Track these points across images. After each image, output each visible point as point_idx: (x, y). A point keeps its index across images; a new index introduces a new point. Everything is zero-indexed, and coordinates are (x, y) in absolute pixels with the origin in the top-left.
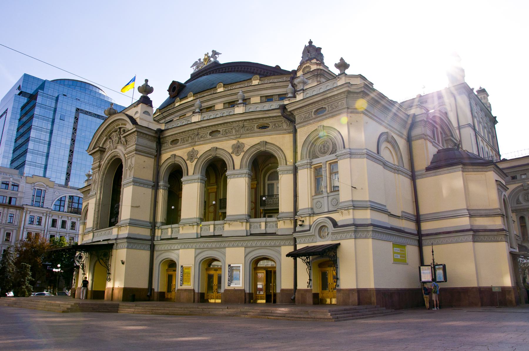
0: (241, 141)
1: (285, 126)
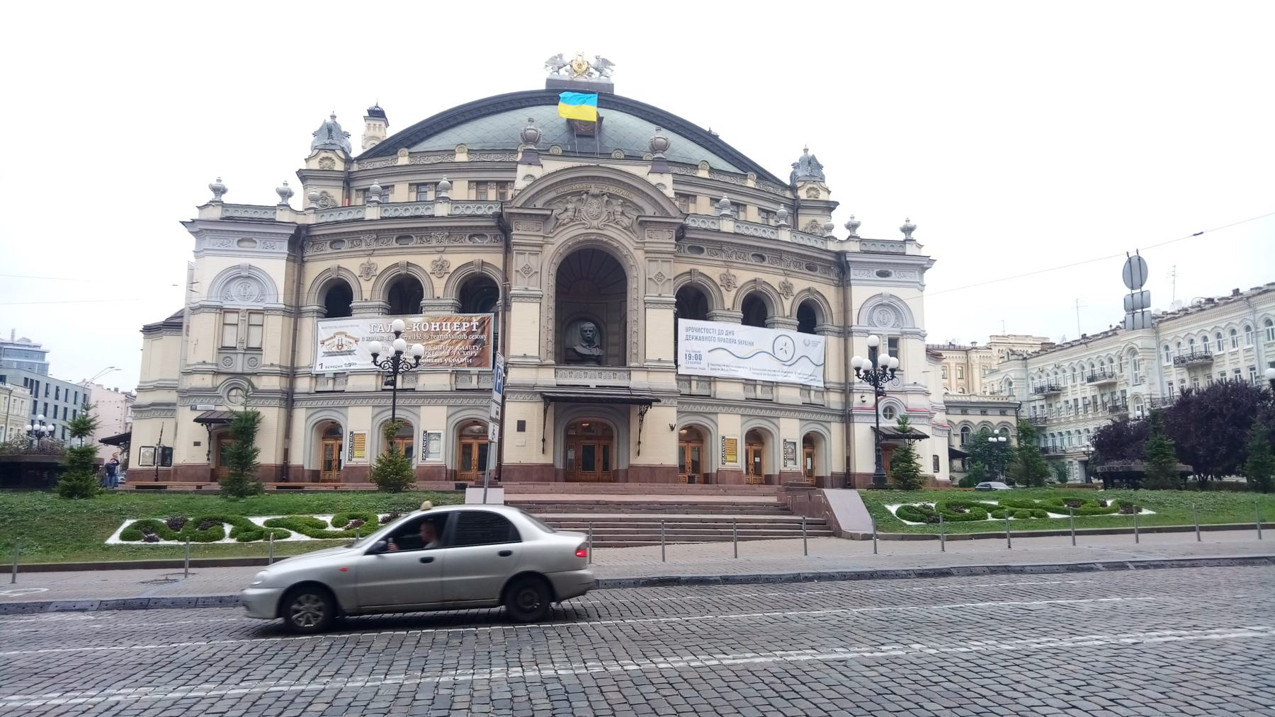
0: (791, 280)
1: (833, 276)
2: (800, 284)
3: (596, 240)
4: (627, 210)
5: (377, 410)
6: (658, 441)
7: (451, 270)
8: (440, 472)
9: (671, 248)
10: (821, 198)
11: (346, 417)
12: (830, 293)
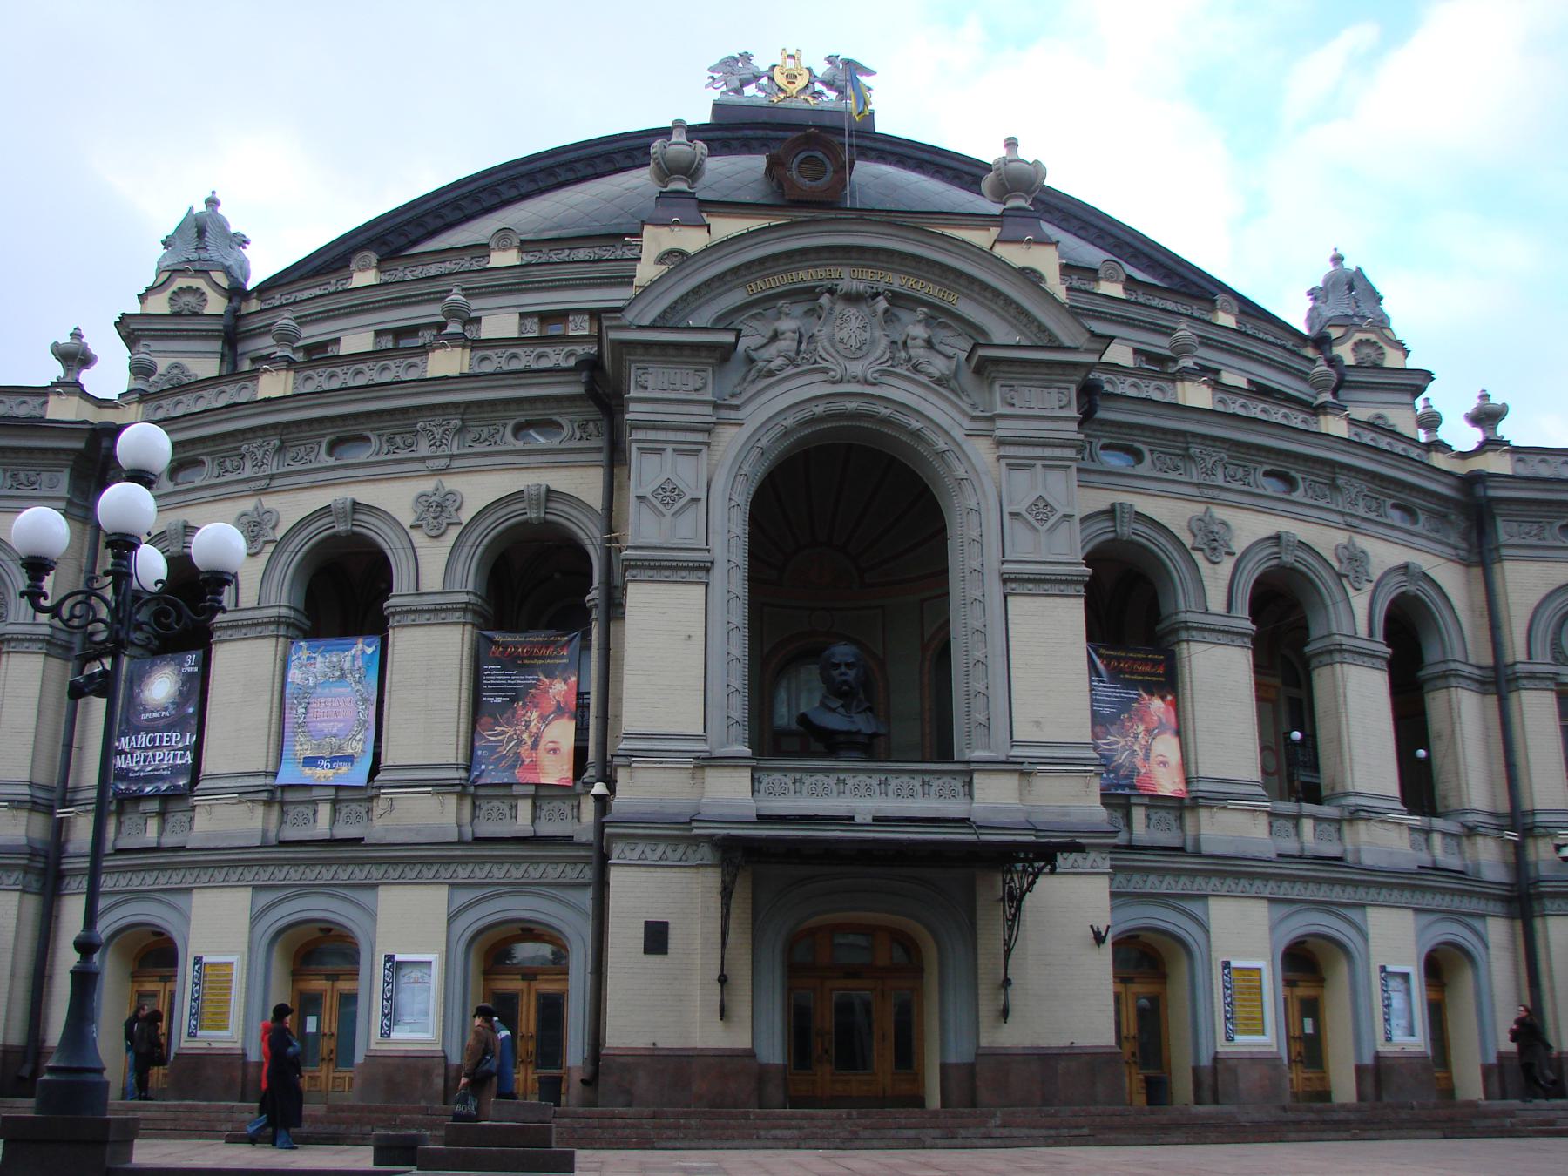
0: (1362, 542)
1: (1453, 539)
2: (1384, 554)
3: (859, 415)
4: (943, 336)
5: (266, 898)
6: (1058, 978)
7: (466, 516)
8: (427, 1073)
9: (1071, 431)
10: (1387, 364)
11: (187, 919)
12: (1451, 578)
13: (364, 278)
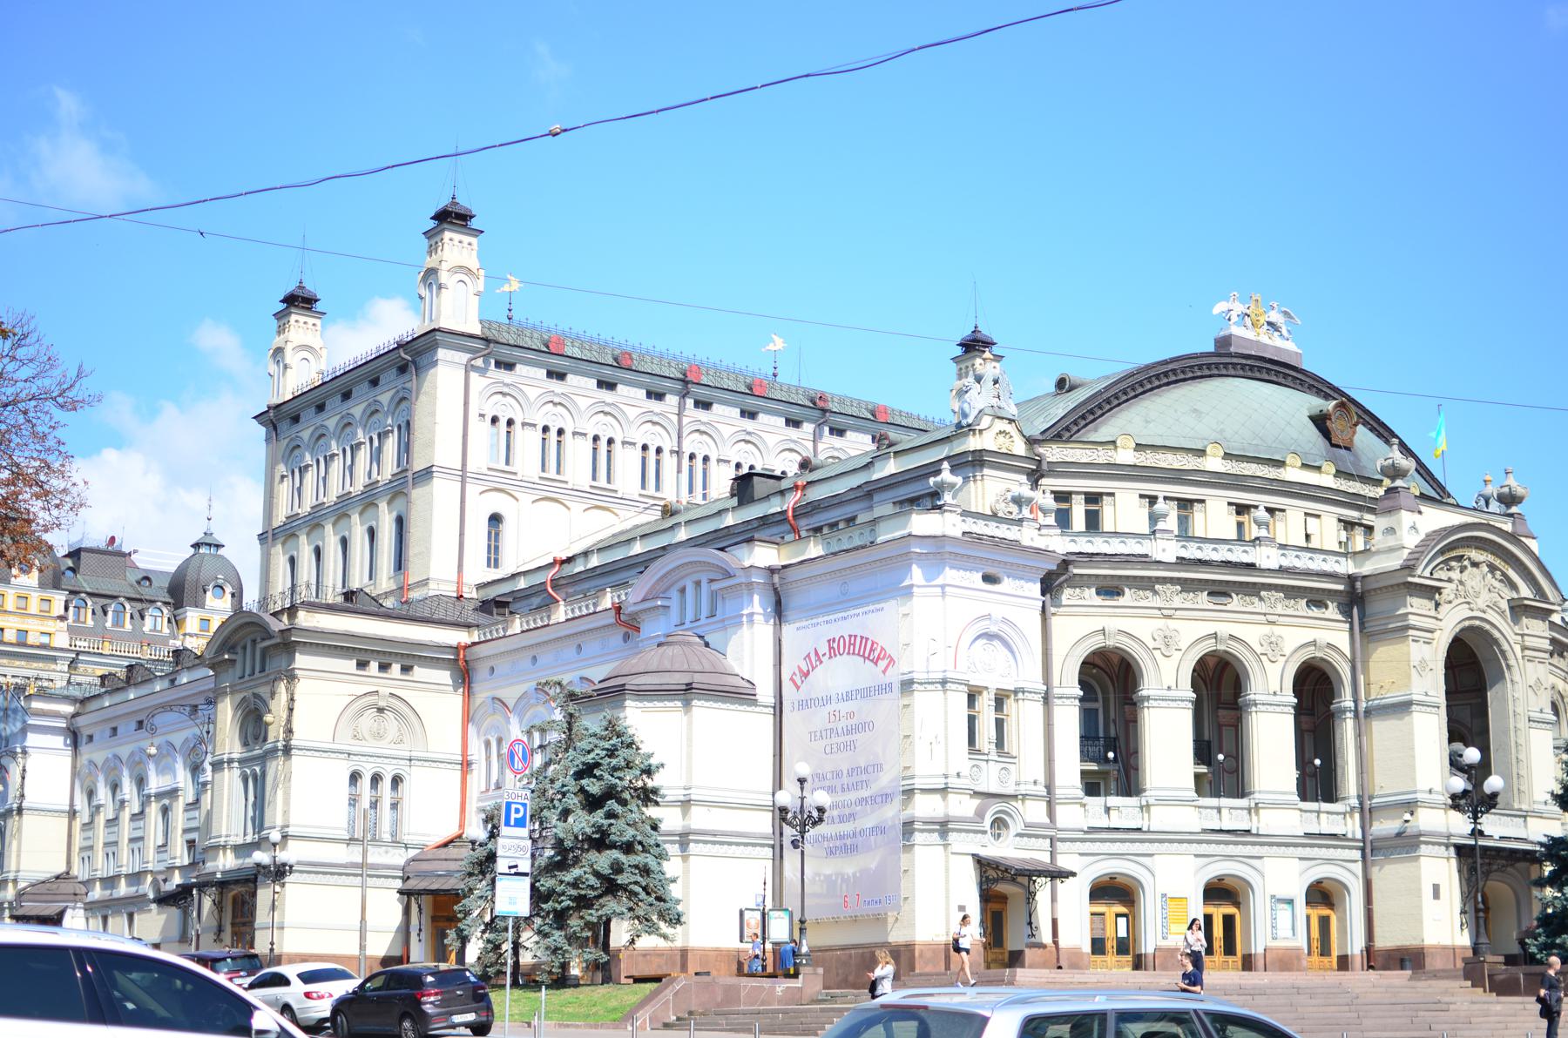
7: (1288, 652)
13: (1125, 456)
